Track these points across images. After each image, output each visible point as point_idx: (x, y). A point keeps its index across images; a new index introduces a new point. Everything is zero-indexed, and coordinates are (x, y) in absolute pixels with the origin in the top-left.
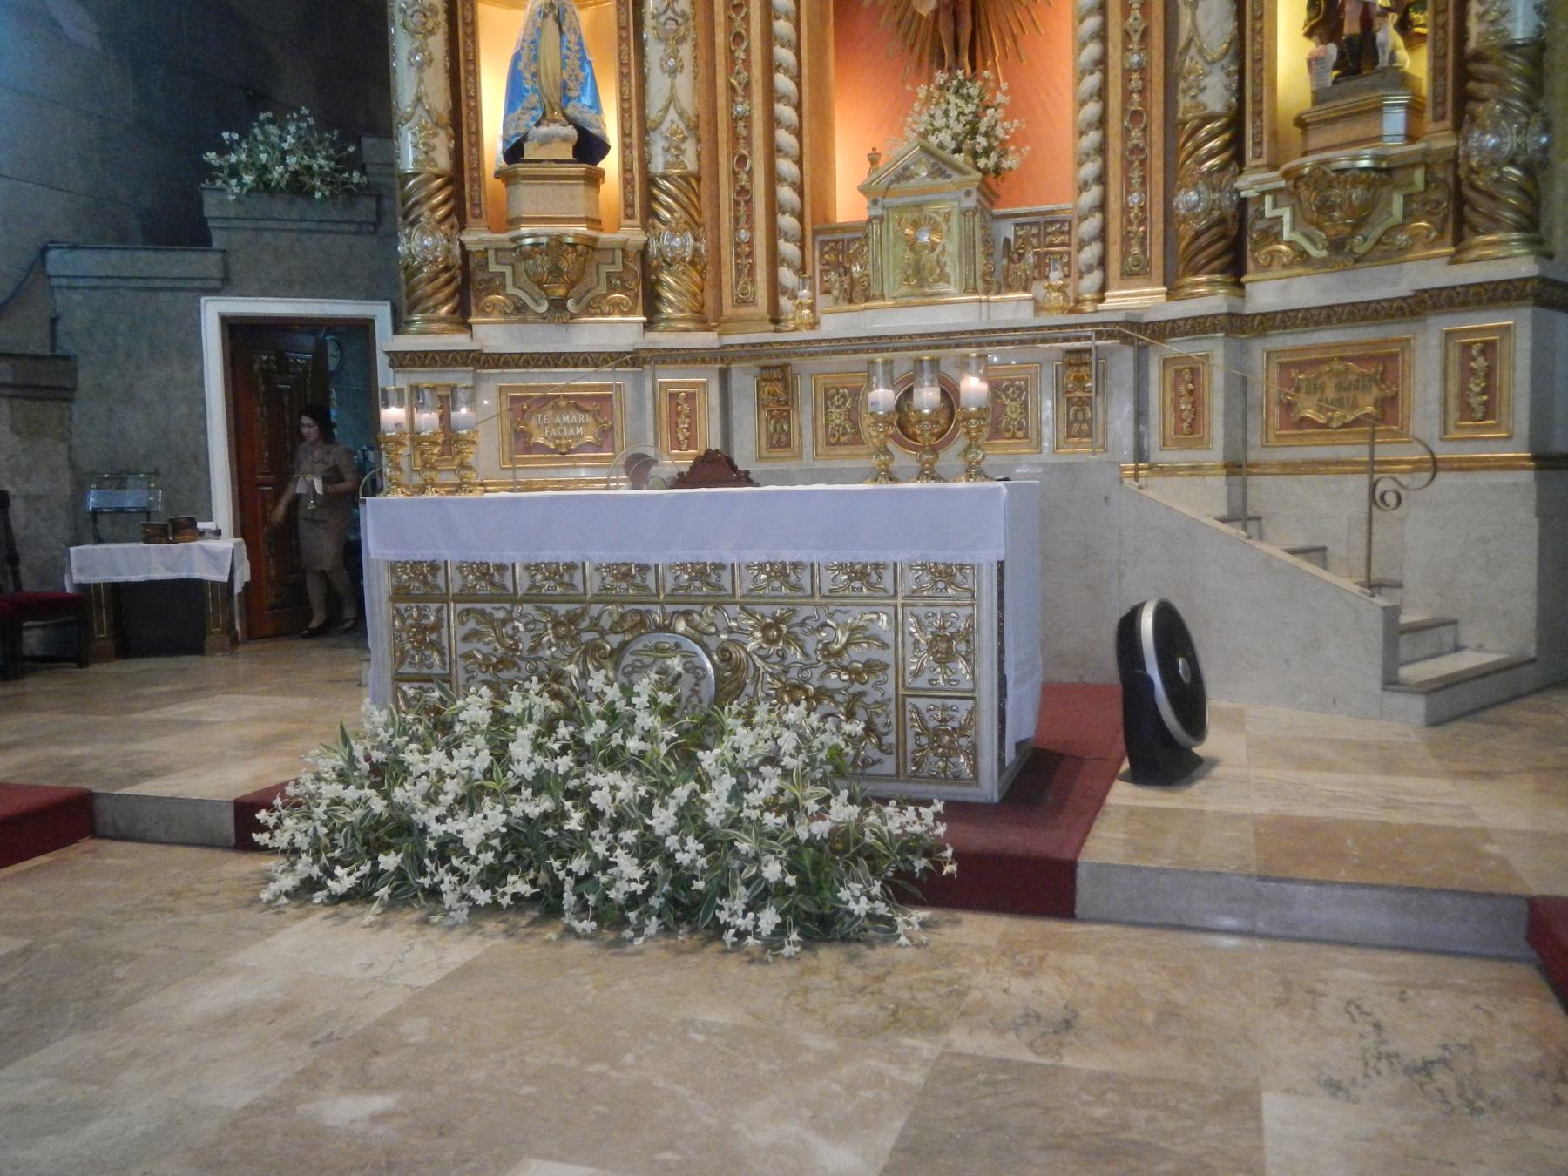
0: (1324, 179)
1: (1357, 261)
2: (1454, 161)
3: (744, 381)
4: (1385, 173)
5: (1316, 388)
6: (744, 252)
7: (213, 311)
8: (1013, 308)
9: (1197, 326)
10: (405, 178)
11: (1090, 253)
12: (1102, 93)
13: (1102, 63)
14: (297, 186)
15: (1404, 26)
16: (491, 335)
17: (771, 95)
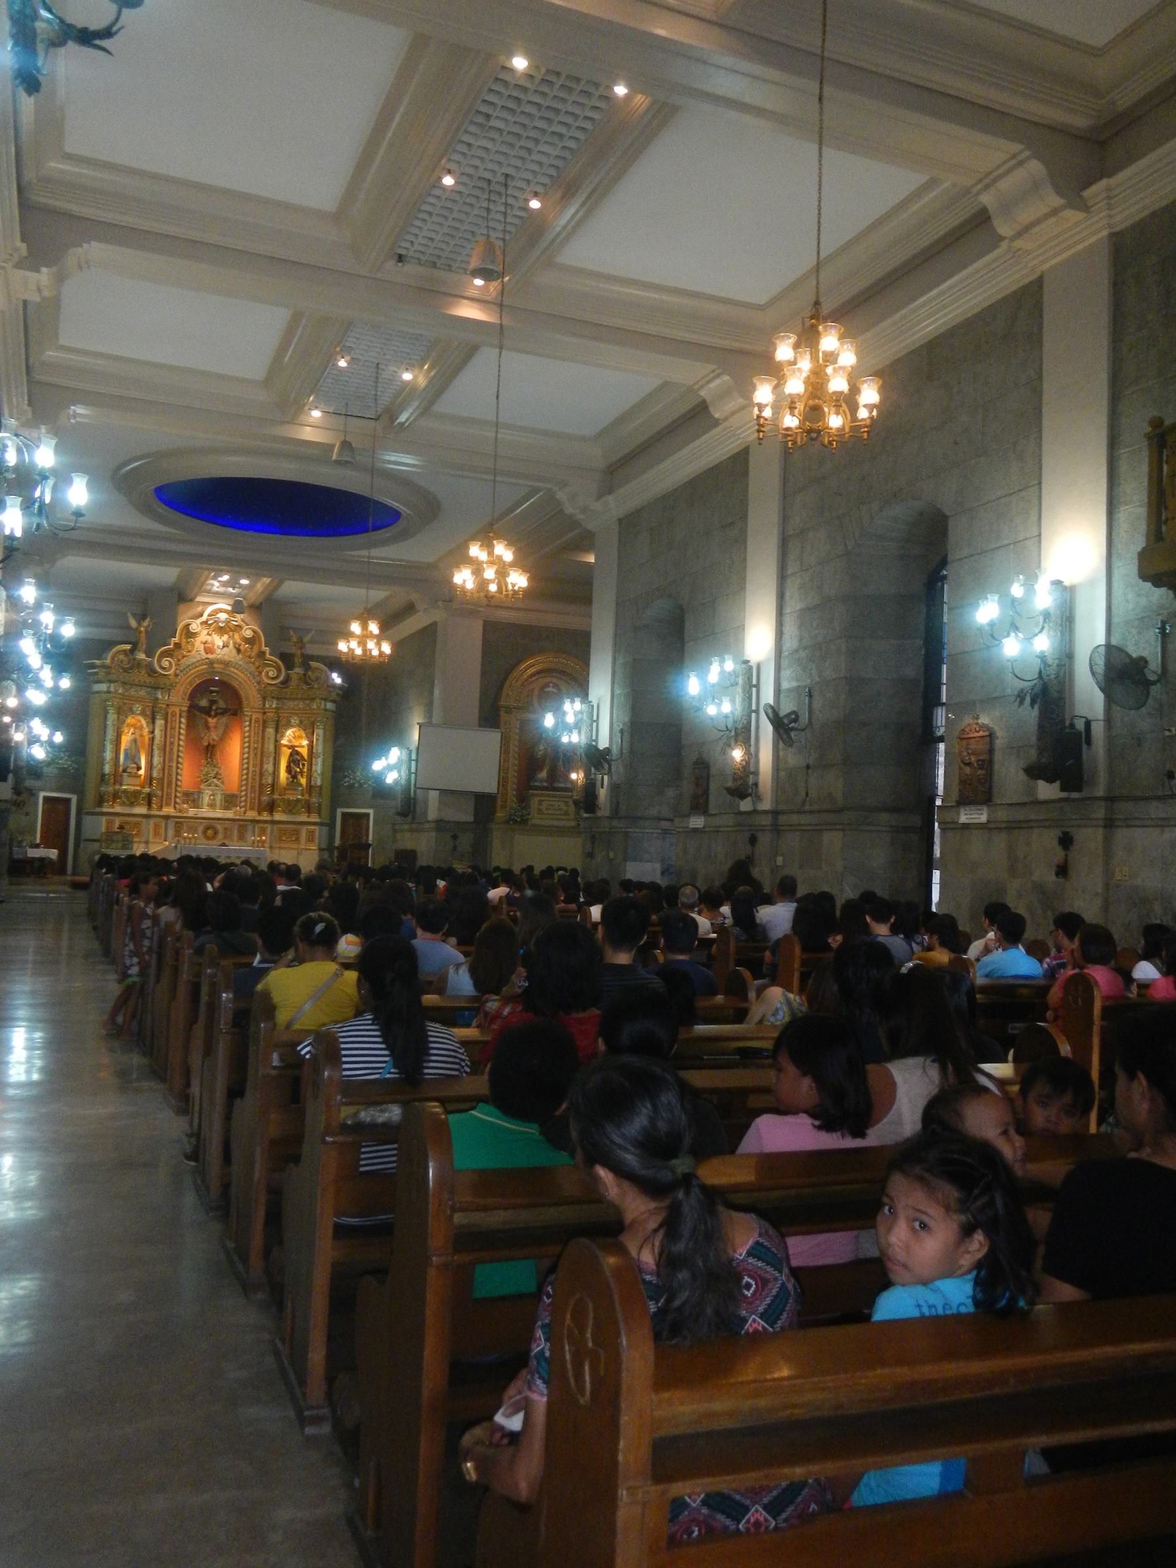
0: (288, 800)
1: (294, 814)
2: (309, 801)
3: (171, 824)
4: (298, 801)
5: (285, 834)
6: (169, 795)
7: (42, 794)
8: (229, 814)
9: (266, 822)
10: (103, 775)
11: (243, 804)
12: (247, 774)
13: (248, 768)
14: (64, 769)
15: (302, 776)
16: (118, 809)
17: (178, 763)
